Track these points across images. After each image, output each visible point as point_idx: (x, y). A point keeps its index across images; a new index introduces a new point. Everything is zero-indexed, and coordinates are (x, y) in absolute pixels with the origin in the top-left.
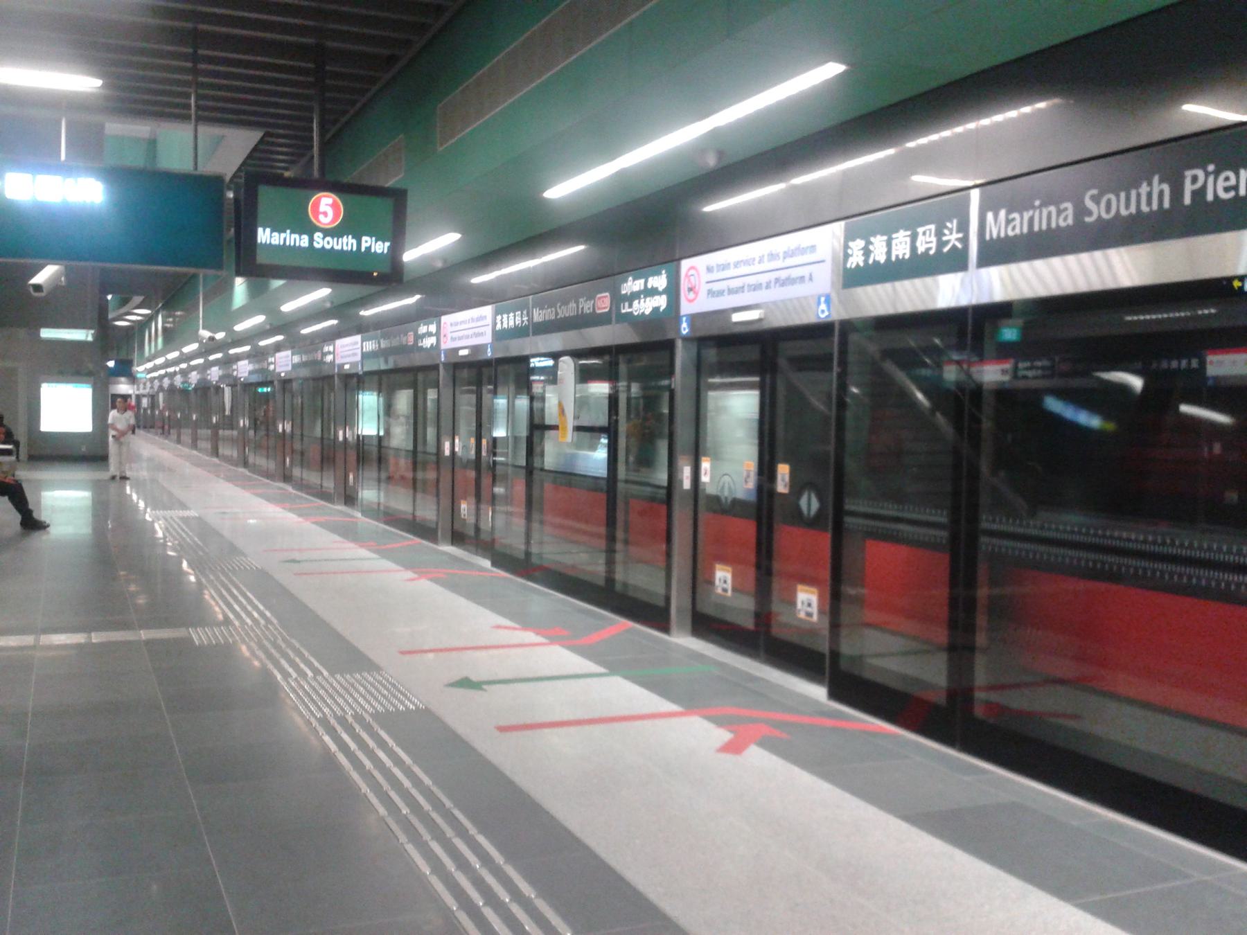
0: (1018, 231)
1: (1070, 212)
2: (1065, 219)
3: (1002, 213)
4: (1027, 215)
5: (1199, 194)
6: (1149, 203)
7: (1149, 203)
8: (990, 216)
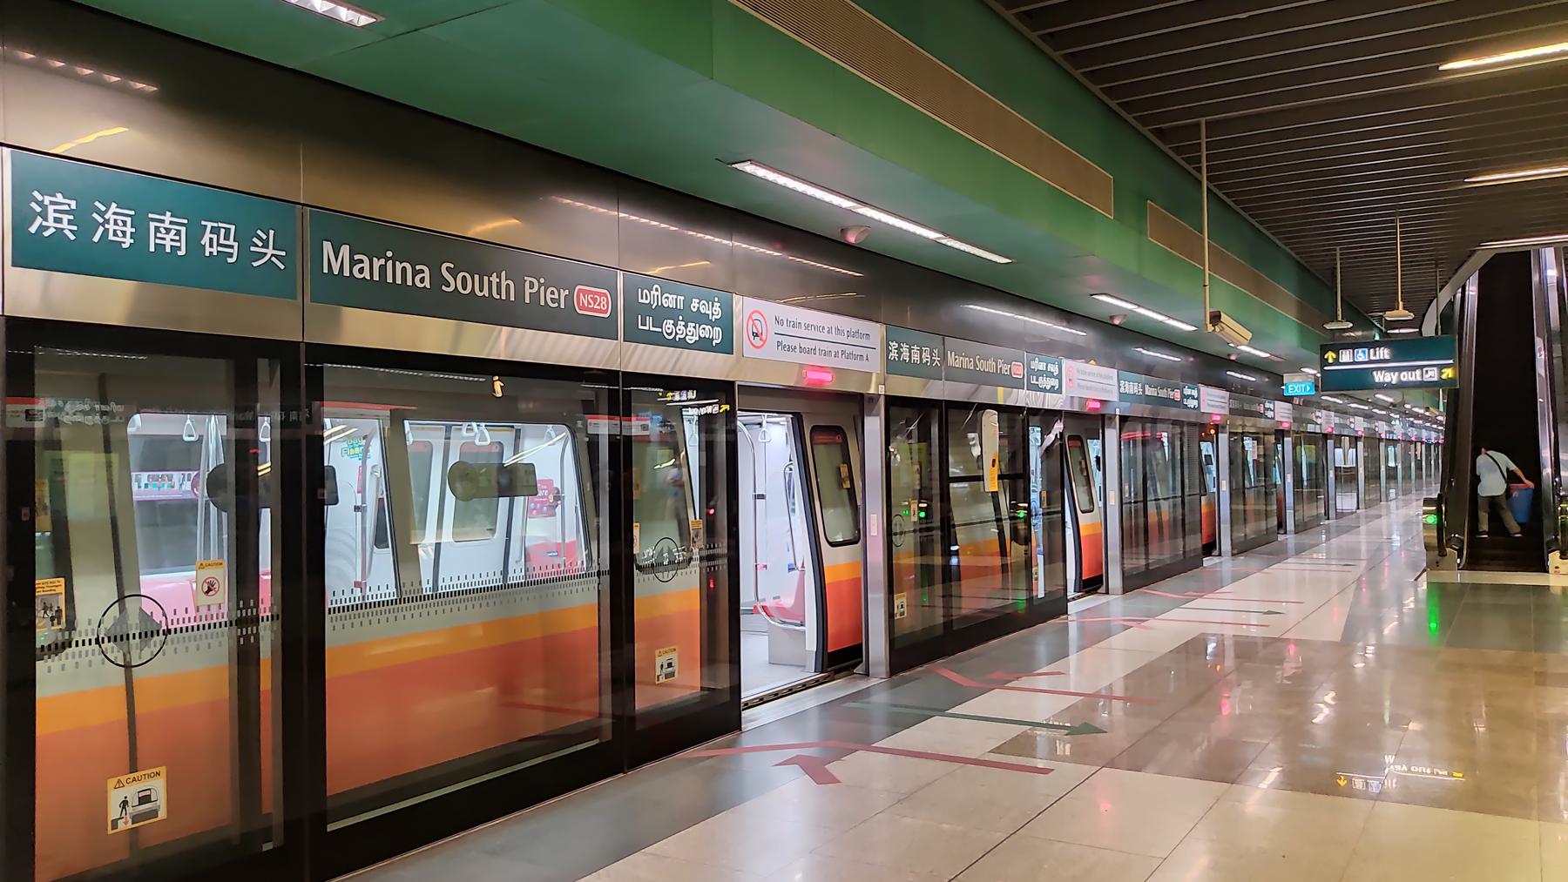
0: (367, 275)
1: (427, 275)
2: (422, 280)
3: (345, 250)
4: (377, 263)
5: (535, 296)
6: (499, 293)
7: (499, 293)
8: (327, 246)
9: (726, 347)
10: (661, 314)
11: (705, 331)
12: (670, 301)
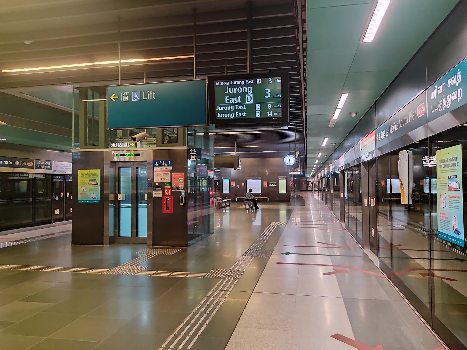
9: (51, 169)
10: (40, 165)
11: (48, 167)
12: (42, 163)
